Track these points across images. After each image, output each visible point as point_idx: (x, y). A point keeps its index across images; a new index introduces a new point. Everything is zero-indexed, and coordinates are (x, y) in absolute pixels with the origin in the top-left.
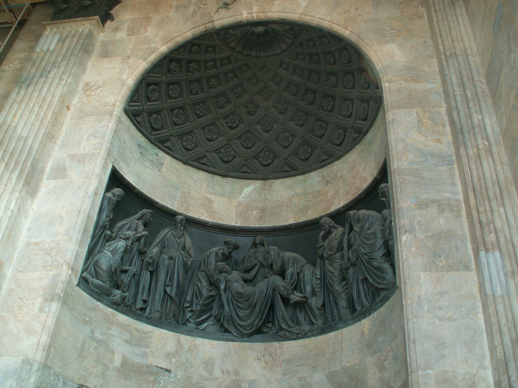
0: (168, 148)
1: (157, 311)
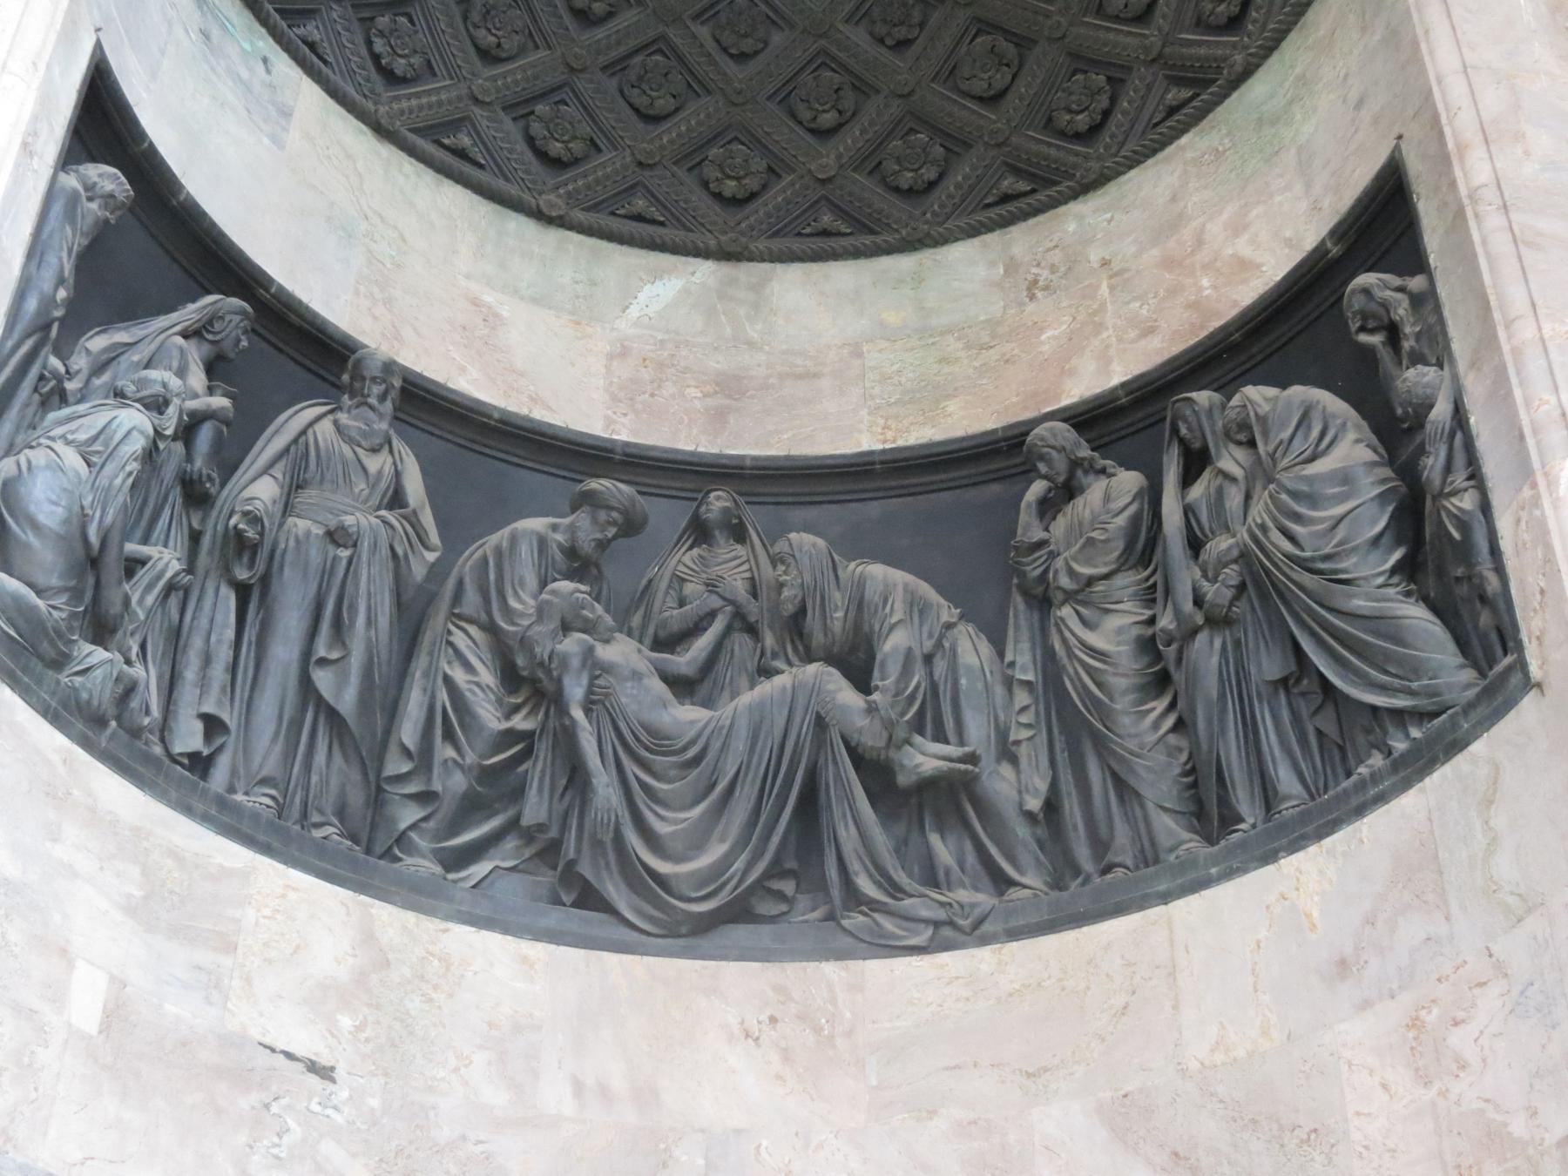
0: (312, 46)
1: (264, 782)
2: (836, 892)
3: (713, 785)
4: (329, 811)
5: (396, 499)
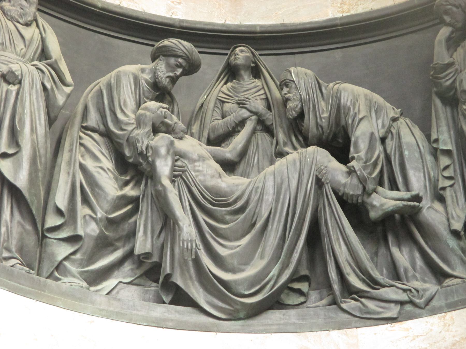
2: (336, 287)
3: (254, 225)
4: (14, 249)
5: (44, 54)
